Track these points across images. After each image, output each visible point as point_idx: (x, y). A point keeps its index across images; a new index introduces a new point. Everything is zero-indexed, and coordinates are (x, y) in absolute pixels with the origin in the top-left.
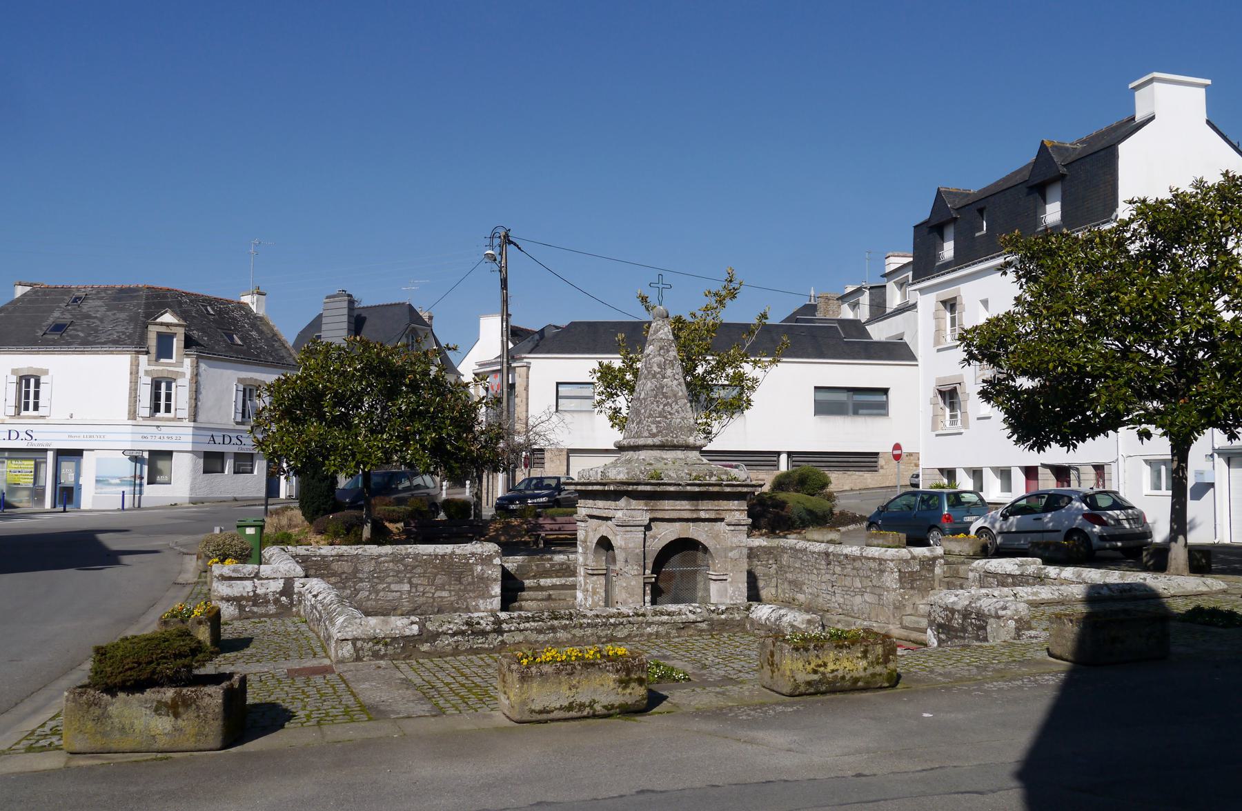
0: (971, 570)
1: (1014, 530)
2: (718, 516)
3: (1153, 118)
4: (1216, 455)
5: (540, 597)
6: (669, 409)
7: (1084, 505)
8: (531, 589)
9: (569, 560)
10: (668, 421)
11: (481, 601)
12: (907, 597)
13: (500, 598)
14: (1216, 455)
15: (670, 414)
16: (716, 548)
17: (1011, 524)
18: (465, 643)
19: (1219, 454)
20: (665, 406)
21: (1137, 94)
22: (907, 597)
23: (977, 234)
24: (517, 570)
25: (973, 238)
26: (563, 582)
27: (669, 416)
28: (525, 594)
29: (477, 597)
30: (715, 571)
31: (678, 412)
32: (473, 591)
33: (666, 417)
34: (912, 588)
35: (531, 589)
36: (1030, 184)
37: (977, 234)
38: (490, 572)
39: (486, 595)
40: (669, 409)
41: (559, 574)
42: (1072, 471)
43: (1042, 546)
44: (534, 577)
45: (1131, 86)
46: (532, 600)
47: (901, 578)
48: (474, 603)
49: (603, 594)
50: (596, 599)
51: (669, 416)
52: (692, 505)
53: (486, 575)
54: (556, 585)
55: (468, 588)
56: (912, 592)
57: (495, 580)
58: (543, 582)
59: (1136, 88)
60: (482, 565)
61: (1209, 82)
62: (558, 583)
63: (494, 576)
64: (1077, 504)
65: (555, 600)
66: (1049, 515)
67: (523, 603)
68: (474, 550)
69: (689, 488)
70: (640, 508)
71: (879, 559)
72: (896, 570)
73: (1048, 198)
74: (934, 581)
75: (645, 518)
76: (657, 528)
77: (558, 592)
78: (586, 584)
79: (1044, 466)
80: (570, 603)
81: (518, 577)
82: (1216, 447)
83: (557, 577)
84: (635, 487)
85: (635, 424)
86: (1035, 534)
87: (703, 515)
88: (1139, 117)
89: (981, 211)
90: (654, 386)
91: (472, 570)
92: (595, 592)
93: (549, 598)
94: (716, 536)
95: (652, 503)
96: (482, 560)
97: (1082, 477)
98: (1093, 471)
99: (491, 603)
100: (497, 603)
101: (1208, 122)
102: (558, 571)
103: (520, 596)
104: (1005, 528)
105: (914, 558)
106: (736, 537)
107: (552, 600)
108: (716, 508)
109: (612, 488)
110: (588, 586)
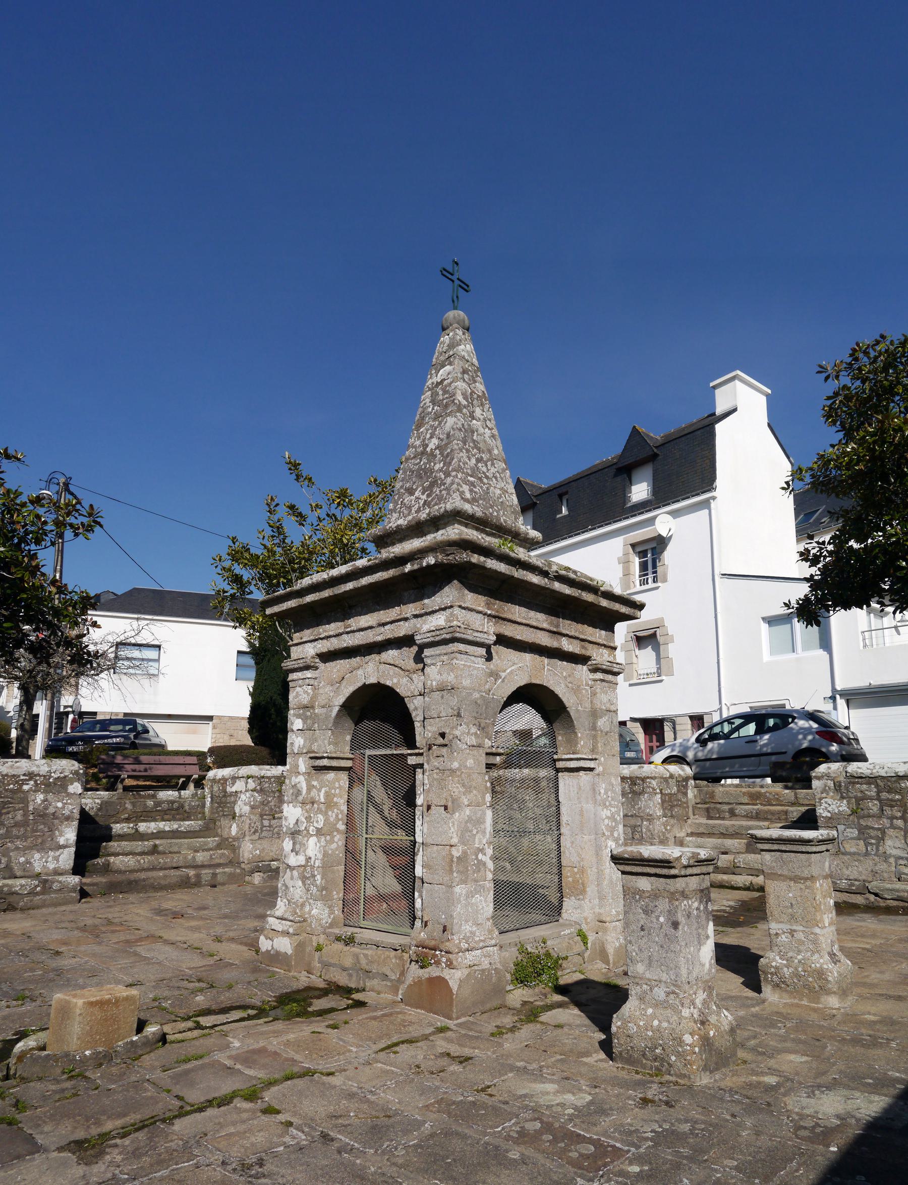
0: (818, 778)
1: (714, 757)
2: (583, 652)
3: (735, 410)
4: (838, 697)
5: (139, 850)
6: (484, 469)
7: (811, 723)
8: (122, 837)
9: (180, 797)
10: (485, 487)
11: (37, 856)
12: (668, 828)
13: (73, 849)
14: (838, 697)
15: (487, 477)
16: (578, 711)
17: (711, 751)
18: (894, 803)
19: (840, 695)
20: (479, 460)
21: (717, 391)
22: (668, 828)
23: (558, 516)
24: (99, 810)
25: (554, 519)
26: (175, 826)
27: (485, 480)
28: (114, 845)
29: (30, 848)
30: (573, 753)
31: (496, 478)
32: (24, 837)
33: (480, 479)
34: (672, 816)
35: (122, 837)
36: (620, 465)
37: (558, 516)
38: (60, 805)
39: (47, 844)
40: (484, 469)
41: (166, 817)
42: (665, 723)
43: (788, 766)
44: (127, 820)
45: (712, 384)
46: (127, 854)
47: (663, 801)
48: (22, 859)
49: (344, 808)
50: (332, 815)
51: (485, 480)
52: (551, 623)
53: (51, 810)
54: (164, 832)
55: (15, 831)
56: (672, 821)
57: (68, 818)
58: (143, 827)
59: (714, 387)
60: (46, 792)
61: (769, 391)
62: (167, 829)
63: (66, 812)
64: (802, 723)
65: (164, 853)
66: (767, 737)
67: (112, 859)
68: (34, 769)
69: (557, 586)
70: (480, 609)
71: (630, 778)
72: (658, 791)
73: (634, 478)
74: (688, 807)
75: (488, 630)
76: (500, 658)
77: (169, 841)
78: (310, 788)
79: (634, 720)
80: (190, 857)
81: (101, 821)
82: (838, 688)
83: (163, 820)
84: (482, 559)
85: (417, 494)
86: (744, 759)
87: (567, 646)
88: (719, 411)
89: (561, 496)
90: (460, 425)
91: (25, 801)
92: (330, 804)
93: (154, 850)
94: (576, 690)
95: (498, 604)
96: (48, 785)
97: (678, 727)
98: (689, 722)
99: (57, 859)
100: (67, 858)
101: (769, 425)
102: (165, 812)
103: (105, 848)
104: (700, 755)
105: (671, 776)
106: (606, 693)
107: (159, 853)
108: (582, 637)
109: (431, 560)
110: (314, 793)
